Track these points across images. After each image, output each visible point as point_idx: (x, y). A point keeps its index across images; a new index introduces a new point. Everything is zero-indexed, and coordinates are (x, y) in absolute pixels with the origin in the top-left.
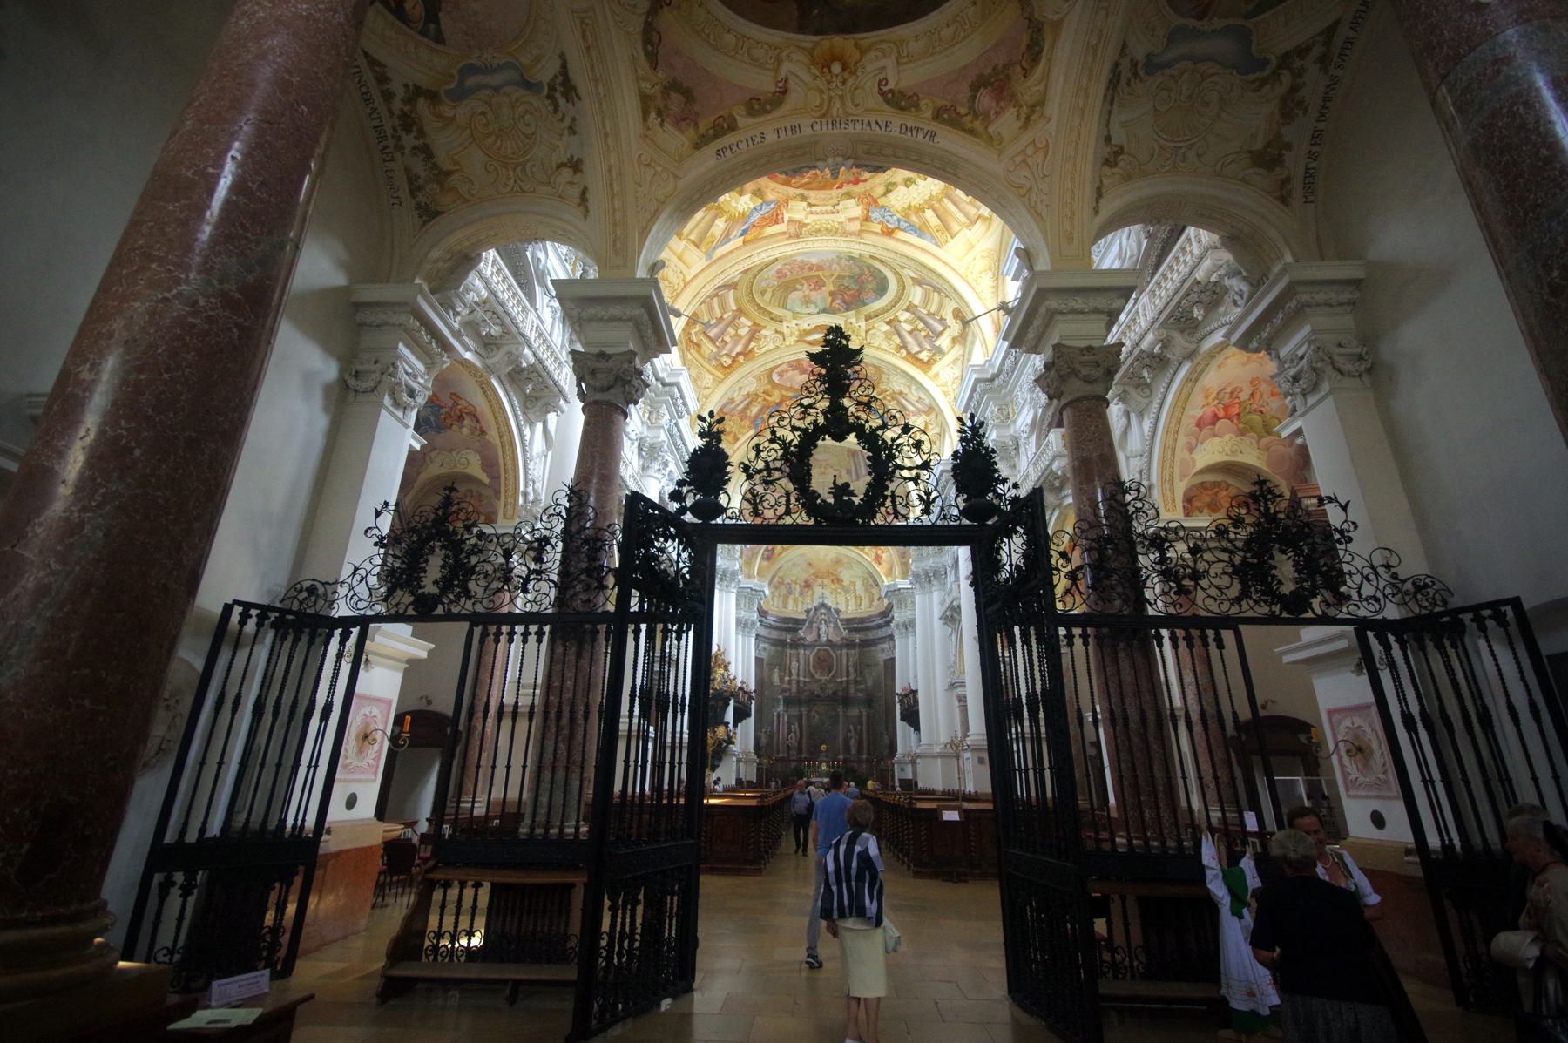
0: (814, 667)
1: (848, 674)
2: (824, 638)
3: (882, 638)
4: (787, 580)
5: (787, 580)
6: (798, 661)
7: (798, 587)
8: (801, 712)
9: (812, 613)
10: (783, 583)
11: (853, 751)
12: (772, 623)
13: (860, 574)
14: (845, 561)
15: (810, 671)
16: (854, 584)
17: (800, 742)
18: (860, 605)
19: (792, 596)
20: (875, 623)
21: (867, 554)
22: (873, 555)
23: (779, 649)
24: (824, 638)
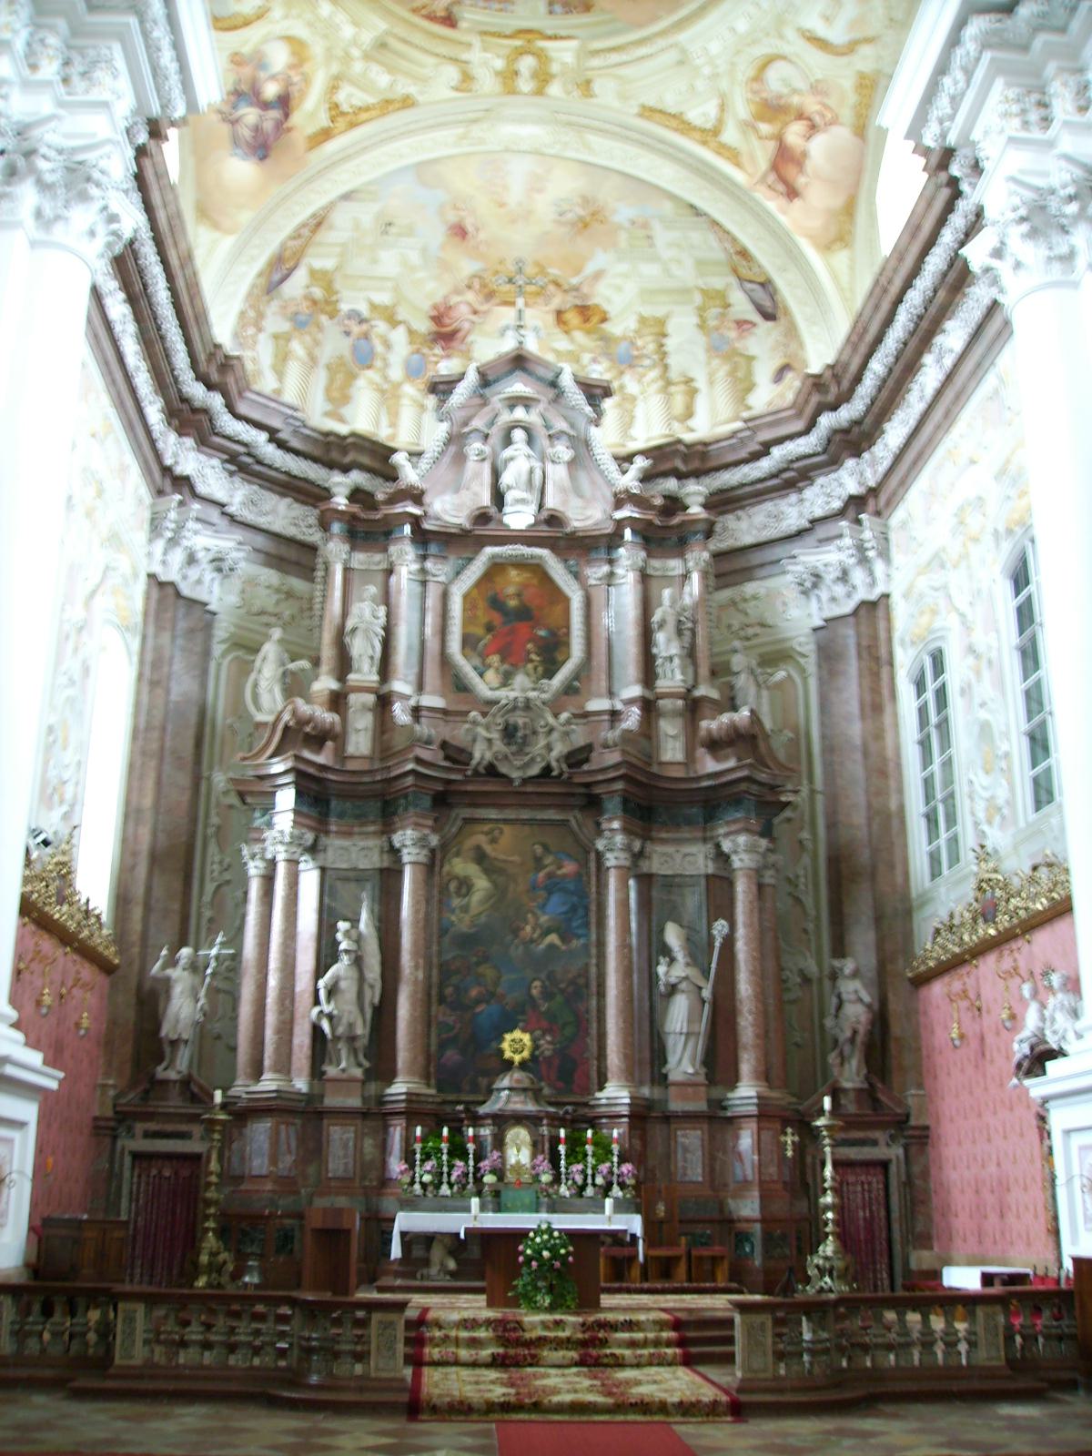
0: (468, 642)
1: (649, 672)
2: (519, 517)
3: (814, 522)
4: (352, 301)
5: (352, 301)
6: (386, 598)
7: (399, 336)
8: (395, 852)
9: (461, 393)
10: (324, 305)
11: (683, 1062)
12: (270, 452)
13: (686, 274)
14: (623, 213)
15: (445, 661)
16: (659, 329)
17: (383, 1015)
18: (689, 413)
19: (370, 374)
20: (777, 452)
21: (733, 156)
22: (763, 155)
23: (297, 584)
24: (519, 517)
